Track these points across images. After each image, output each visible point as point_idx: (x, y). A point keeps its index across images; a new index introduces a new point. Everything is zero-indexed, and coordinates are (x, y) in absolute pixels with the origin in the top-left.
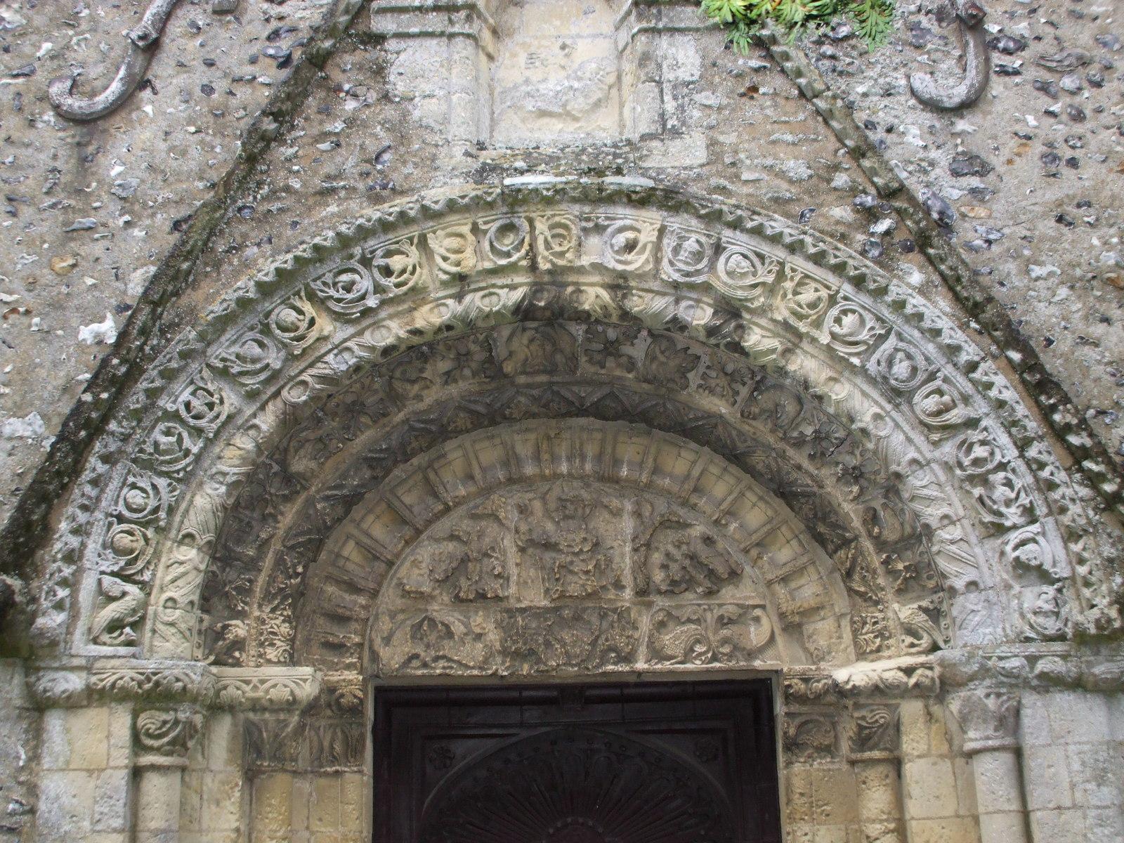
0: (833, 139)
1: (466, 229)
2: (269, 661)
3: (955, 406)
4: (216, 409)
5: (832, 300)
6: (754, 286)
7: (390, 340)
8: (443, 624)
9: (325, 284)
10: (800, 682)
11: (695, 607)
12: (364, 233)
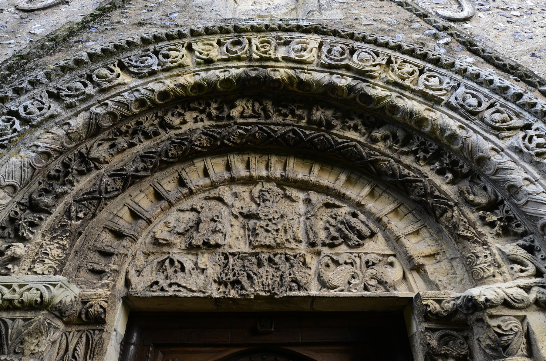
0: (408, 12)
1: (215, 43)
2: (36, 273)
3: (511, 119)
4: (43, 111)
5: (421, 72)
6: (375, 66)
7: (162, 89)
8: (179, 262)
9: (130, 60)
10: (434, 303)
11: (349, 255)
12: (157, 39)
